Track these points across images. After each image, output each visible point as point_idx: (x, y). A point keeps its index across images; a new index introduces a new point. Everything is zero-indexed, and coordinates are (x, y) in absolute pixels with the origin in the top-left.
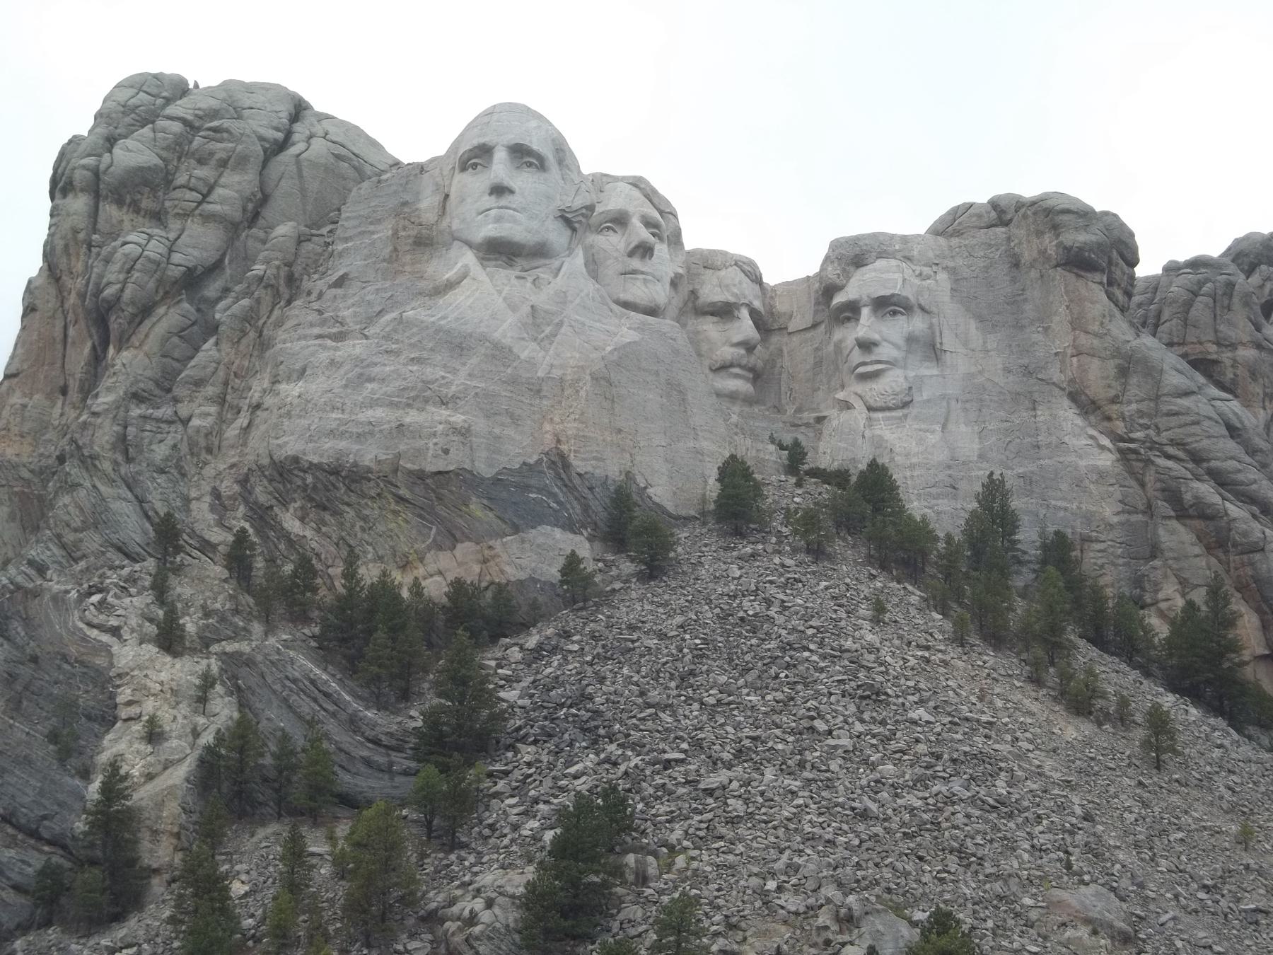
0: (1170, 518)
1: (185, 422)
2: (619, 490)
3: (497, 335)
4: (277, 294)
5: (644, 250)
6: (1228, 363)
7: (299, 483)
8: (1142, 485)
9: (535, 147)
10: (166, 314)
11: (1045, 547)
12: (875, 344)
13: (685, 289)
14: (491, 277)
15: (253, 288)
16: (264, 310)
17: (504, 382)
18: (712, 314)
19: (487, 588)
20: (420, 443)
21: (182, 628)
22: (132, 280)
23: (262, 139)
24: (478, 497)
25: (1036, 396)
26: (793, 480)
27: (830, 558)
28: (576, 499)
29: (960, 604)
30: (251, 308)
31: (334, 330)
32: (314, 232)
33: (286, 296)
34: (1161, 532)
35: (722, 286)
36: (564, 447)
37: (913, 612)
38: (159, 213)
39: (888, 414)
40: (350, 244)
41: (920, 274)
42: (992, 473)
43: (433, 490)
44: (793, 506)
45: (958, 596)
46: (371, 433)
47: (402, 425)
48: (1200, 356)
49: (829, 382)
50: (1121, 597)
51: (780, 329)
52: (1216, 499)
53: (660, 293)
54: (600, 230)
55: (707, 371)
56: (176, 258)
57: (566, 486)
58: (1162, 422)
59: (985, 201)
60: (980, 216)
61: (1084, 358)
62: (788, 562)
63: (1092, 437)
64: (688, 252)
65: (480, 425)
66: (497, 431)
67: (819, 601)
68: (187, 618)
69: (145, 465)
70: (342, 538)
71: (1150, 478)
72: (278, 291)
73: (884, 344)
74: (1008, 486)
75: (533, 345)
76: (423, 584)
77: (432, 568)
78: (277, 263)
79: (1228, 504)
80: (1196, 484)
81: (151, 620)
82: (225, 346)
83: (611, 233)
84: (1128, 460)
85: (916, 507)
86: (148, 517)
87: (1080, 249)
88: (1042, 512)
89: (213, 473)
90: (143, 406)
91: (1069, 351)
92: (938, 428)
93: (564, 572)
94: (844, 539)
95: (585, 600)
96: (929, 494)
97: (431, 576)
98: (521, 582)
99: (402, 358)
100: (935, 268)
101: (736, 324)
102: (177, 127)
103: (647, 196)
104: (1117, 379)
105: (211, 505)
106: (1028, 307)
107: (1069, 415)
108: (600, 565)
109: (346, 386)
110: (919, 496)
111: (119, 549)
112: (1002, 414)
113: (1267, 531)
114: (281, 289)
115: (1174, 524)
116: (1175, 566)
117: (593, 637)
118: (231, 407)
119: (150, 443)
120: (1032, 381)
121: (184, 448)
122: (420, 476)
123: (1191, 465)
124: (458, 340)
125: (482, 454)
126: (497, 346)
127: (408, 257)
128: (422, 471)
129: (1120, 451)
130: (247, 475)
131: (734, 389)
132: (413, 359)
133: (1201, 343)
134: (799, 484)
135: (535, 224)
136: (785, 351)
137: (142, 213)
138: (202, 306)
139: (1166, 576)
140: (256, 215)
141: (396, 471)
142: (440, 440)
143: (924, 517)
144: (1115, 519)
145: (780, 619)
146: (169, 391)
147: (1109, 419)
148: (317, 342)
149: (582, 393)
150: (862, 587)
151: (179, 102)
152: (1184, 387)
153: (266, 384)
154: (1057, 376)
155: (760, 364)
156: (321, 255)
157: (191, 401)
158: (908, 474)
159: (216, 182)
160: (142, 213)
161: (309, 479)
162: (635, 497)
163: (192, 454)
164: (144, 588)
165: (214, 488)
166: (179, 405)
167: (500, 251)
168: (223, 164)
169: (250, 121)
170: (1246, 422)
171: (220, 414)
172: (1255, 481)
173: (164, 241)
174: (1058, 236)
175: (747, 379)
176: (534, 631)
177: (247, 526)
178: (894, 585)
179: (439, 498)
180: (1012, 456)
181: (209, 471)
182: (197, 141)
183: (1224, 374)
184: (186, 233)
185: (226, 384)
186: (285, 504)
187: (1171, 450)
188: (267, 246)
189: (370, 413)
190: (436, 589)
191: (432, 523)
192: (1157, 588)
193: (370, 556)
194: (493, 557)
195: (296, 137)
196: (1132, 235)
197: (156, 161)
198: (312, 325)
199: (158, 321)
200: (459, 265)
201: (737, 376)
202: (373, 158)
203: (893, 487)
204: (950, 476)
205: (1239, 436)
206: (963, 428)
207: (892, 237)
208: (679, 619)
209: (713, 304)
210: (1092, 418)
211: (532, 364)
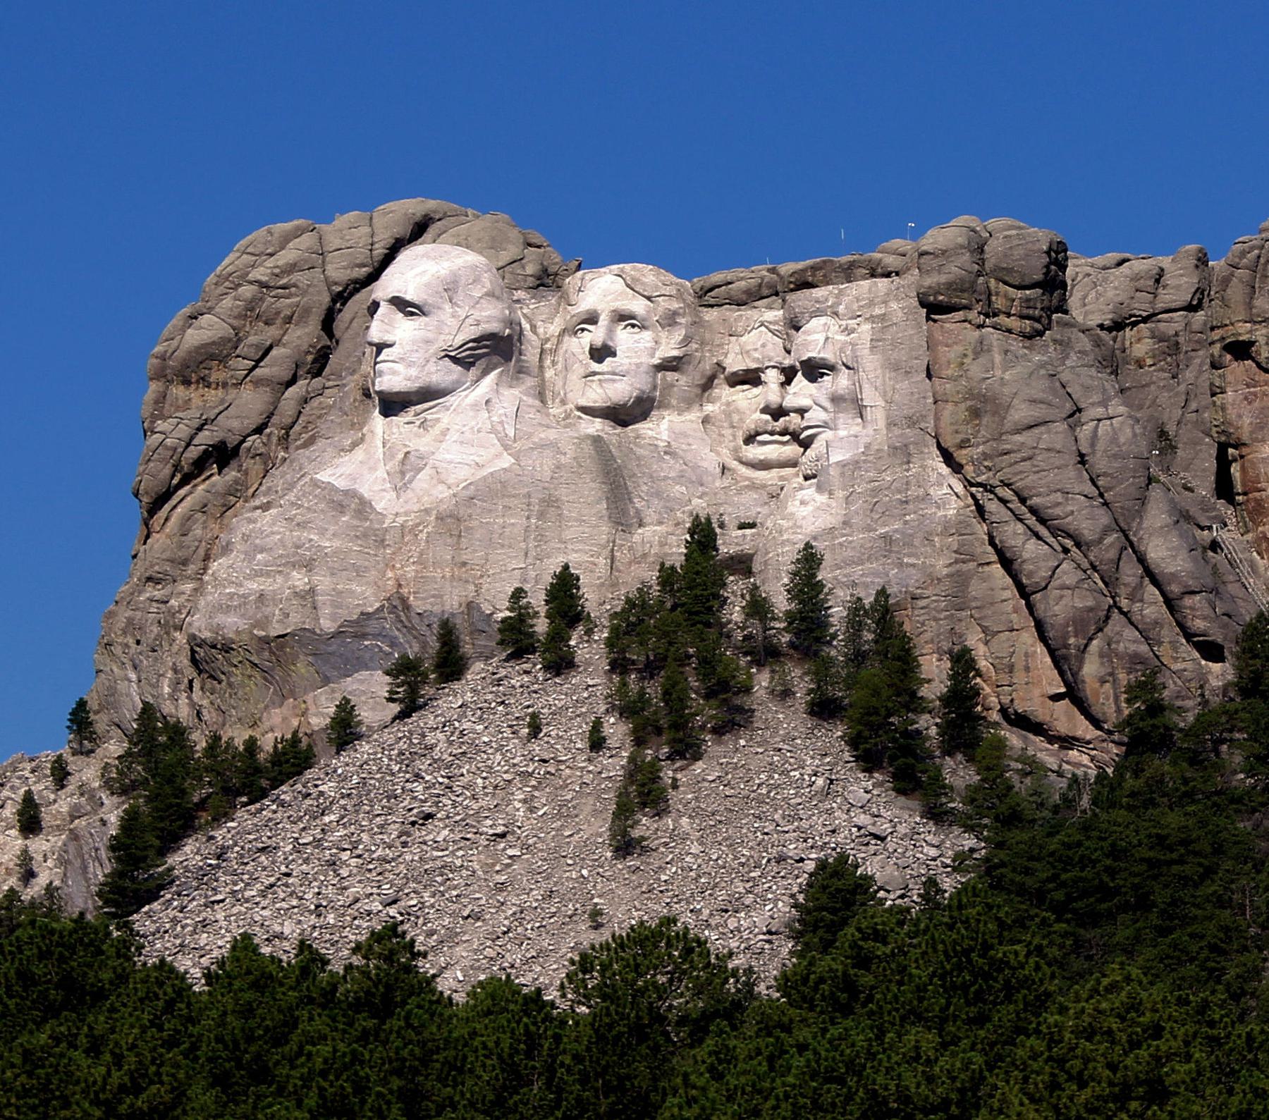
0: (988, 564)
9: (408, 298)
35: (744, 352)
36: (405, 591)
53: (621, 391)
73: (815, 407)
111: (119, 726)
122: (266, 641)
123: (1016, 505)
126: (361, 498)
128: (267, 636)
135: (413, 372)
137: (214, 386)
144: (945, 571)
147: (961, 466)
160: (214, 386)
164: (46, 776)
168: (289, 320)
172: (1072, 512)
209: (734, 374)
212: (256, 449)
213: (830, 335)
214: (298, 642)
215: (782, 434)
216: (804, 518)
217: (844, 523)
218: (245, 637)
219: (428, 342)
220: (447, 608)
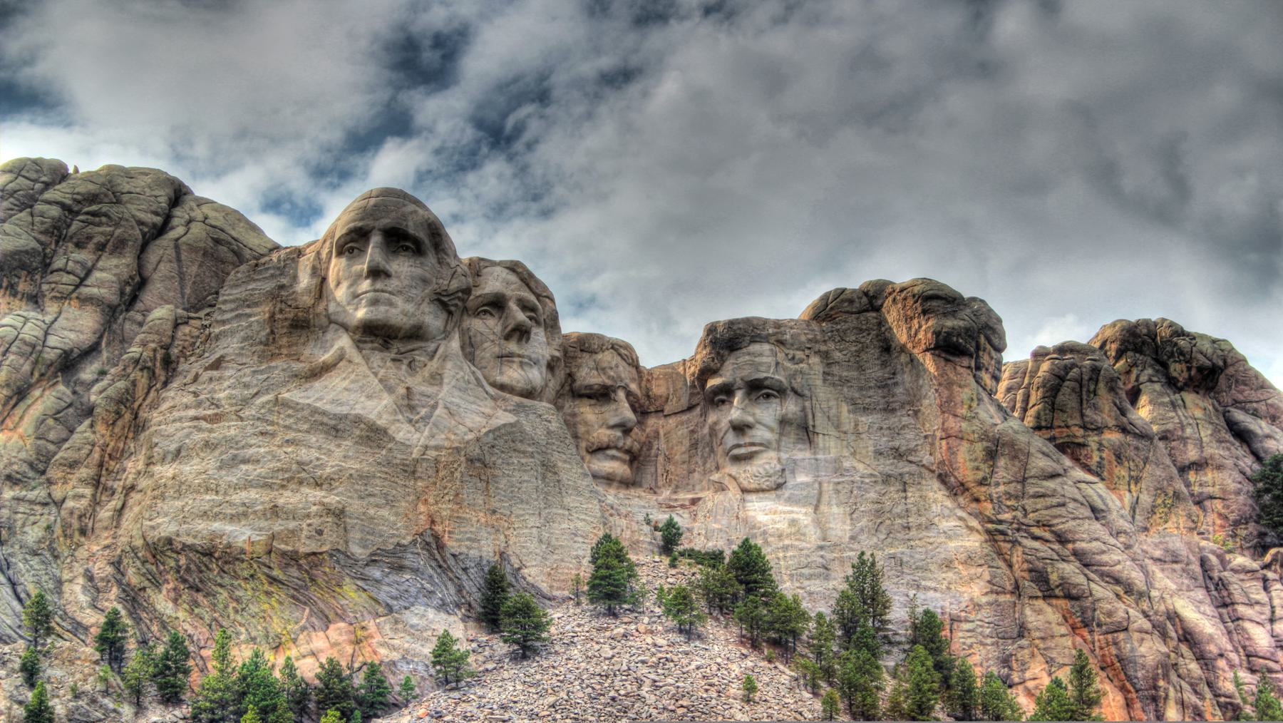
0: (1037, 597)
1: (59, 504)
2: (493, 571)
3: (372, 417)
4: (153, 376)
5: (521, 333)
6: (1094, 446)
7: (173, 564)
8: (1010, 566)
9: (411, 231)
10: (41, 396)
11: (915, 627)
12: (749, 426)
13: (561, 373)
14: (367, 359)
15: (129, 370)
16: (140, 392)
17: (379, 464)
18: (589, 397)
19: (360, 668)
20: (292, 525)
21: (49, 710)
22: (7, 362)
23: (140, 223)
24: (354, 578)
25: (906, 477)
26: (666, 561)
27: (700, 637)
28: (451, 579)
29: (831, 684)
30: (127, 391)
31: (210, 412)
32: (192, 315)
33: (163, 378)
34: (1028, 611)
35: (599, 368)
36: (439, 528)
37: (783, 691)
38: (36, 296)
39: (761, 495)
40: (227, 327)
41: (793, 358)
42: (863, 553)
44: (666, 587)
45: (828, 673)
46: (245, 515)
47: (276, 506)
48: (1066, 440)
49: (704, 464)
50: (989, 677)
52: (1081, 579)
53: (536, 376)
54: (477, 313)
56: (52, 341)
57: (440, 567)
58: (1029, 503)
59: (857, 287)
60: (851, 301)
61: (950, 441)
62: (660, 641)
63: (961, 519)
64: (565, 336)
65: (355, 506)
66: (372, 512)
67: (691, 680)
68: (56, 700)
69: (17, 547)
70: (215, 620)
71: (1017, 558)
72: (154, 373)
73: (758, 426)
74: (879, 566)
75: (407, 427)
76: (296, 664)
77: (304, 649)
78: (153, 345)
79: (1093, 585)
80: (1064, 565)
81: (20, 703)
82: (101, 428)
83: (488, 316)
84: (996, 541)
85: (787, 588)
86: (20, 600)
87: (949, 334)
88: (912, 593)
89: (86, 554)
90: (17, 488)
91: (938, 434)
92: (811, 510)
93: (437, 655)
94: (717, 620)
95: (458, 681)
96: (801, 575)
97: (304, 657)
98: (394, 663)
99: (278, 440)
100: (807, 352)
101: (613, 406)
102: (55, 211)
103: (522, 280)
104: (985, 461)
105: (84, 587)
106: (899, 390)
107: (937, 495)
108: (474, 645)
109: (220, 468)
110: (792, 576)
112: (872, 495)
113: (1131, 611)
114: (157, 371)
115: (1040, 603)
116: (1042, 646)
117: (465, 718)
118: (105, 489)
119: (24, 525)
120: (901, 464)
121: (58, 530)
122: (292, 558)
123: (1056, 546)
124: (333, 422)
125: (356, 535)
127: (284, 341)
129: (988, 532)
130: (120, 557)
132: (287, 441)
133: (1068, 427)
134: (673, 566)
136: (662, 432)
137: (19, 296)
138: (77, 388)
139: (1033, 655)
140: (134, 298)
141: (270, 552)
142: (315, 521)
143: (794, 596)
144: (984, 600)
145: (651, 699)
146: (43, 473)
148: (195, 423)
149: (457, 474)
150: (734, 667)
151: (57, 187)
152: (1050, 470)
153: (141, 466)
154: (927, 459)
155: (636, 446)
156: (198, 337)
157: (65, 483)
158: (781, 555)
159: (93, 266)
160: (19, 296)
161: (183, 561)
162: (510, 578)
163: (65, 536)
164: (13, 671)
165: (87, 570)
166: (54, 487)
167: (377, 335)
168: (101, 247)
169: (129, 206)
170: (1110, 504)
171: (94, 496)
172: (1119, 562)
173: (39, 323)
174: (927, 320)
175: (624, 461)
176: (406, 711)
177: (119, 607)
178: (765, 664)
179: (312, 580)
180: (883, 537)
181: (82, 553)
182: (75, 225)
183: (1091, 458)
184: (63, 316)
185: (101, 465)
186: (157, 585)
187: (1037, 531)
188: (145, 328)
189: (244, 494)
190: (309, 669)
191: (305, 604)
192: (1024, 667)
193: (242, 637)
194: (366, 638)
195: (175, 221)
196: (999, 321)
197: (34, 244)
198: (187, 407)
199: (33, 403)
200: (336, 347)
201: (613, 458)
202: (252, 241)
203: (764, 571)
204: (822, 557)
205: (1104, 517)
206: (835, 509)
207: (765, 322)
208: (551, 699)
209: (589, 387)
210: (961, 499)
211: (406, 446)
212: (145, 361)
214: (338, 562)
216: (806, 526)
217: (853, 538)
218: (260, 549)
219: (425, 281)
220: (484, 554)
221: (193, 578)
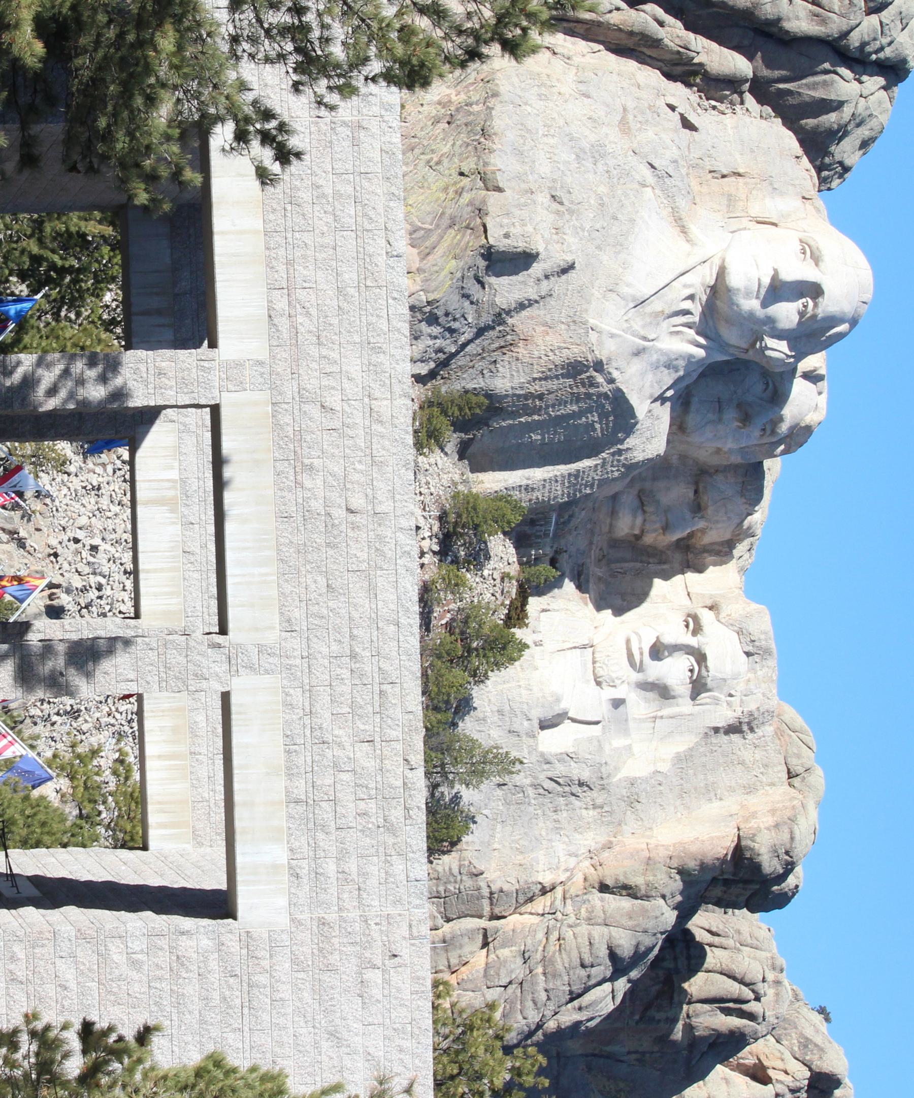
13: (715, 461)
18: (696, 492)
25: (606, 808)
39: (590, 666)
41: (731, 695)
43: (469, 224)
51: (688, 561)
55: (638, 486)
60: (798, 756)
64: (761, 464)
92: (570, 715)
101: (688, 515)
112: (586, 775)
122: (481, 212)
131: (621, 515)
136: (665, 567)
144: (483, 884)
175: (632, 527)
196: (780, 907)
201: (635, 517)
213: (728, 682)
215: (642, 531)
217: (542, 755)
221: (461, 119)
